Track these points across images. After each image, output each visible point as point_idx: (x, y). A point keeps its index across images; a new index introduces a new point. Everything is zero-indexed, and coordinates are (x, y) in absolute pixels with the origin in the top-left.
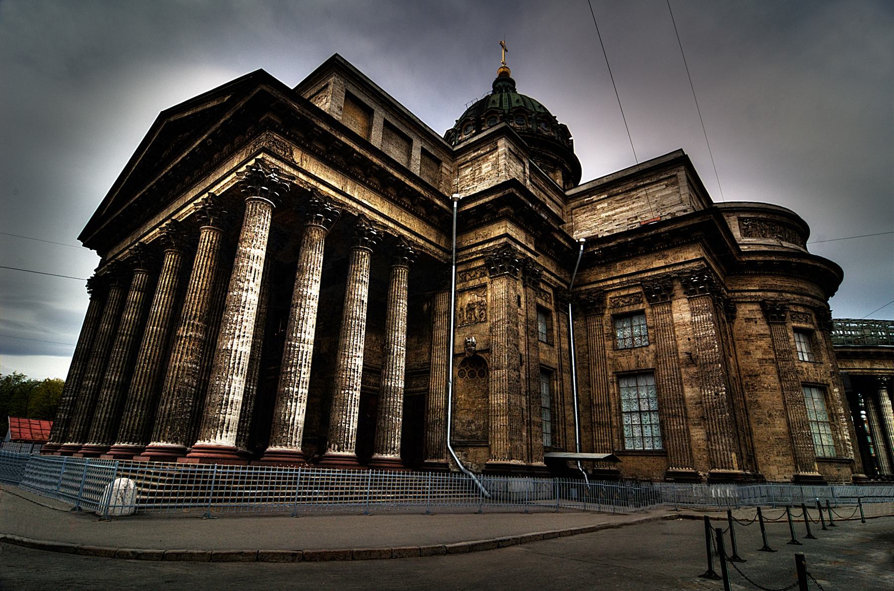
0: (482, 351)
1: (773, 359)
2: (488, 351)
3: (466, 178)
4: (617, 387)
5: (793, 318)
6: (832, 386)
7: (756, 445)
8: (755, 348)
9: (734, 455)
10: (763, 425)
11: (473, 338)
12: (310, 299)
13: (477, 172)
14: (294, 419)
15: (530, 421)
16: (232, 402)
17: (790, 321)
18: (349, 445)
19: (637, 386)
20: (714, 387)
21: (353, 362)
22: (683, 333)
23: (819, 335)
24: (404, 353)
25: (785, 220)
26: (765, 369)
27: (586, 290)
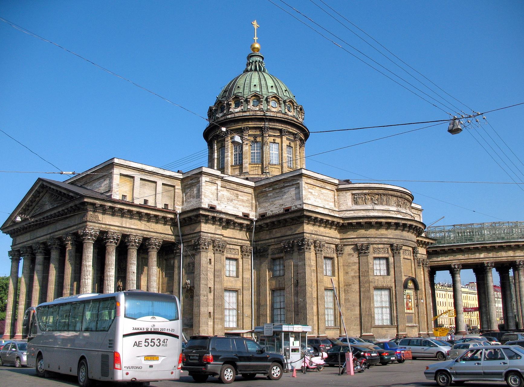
2: (193, 287)
10: (349, 311)
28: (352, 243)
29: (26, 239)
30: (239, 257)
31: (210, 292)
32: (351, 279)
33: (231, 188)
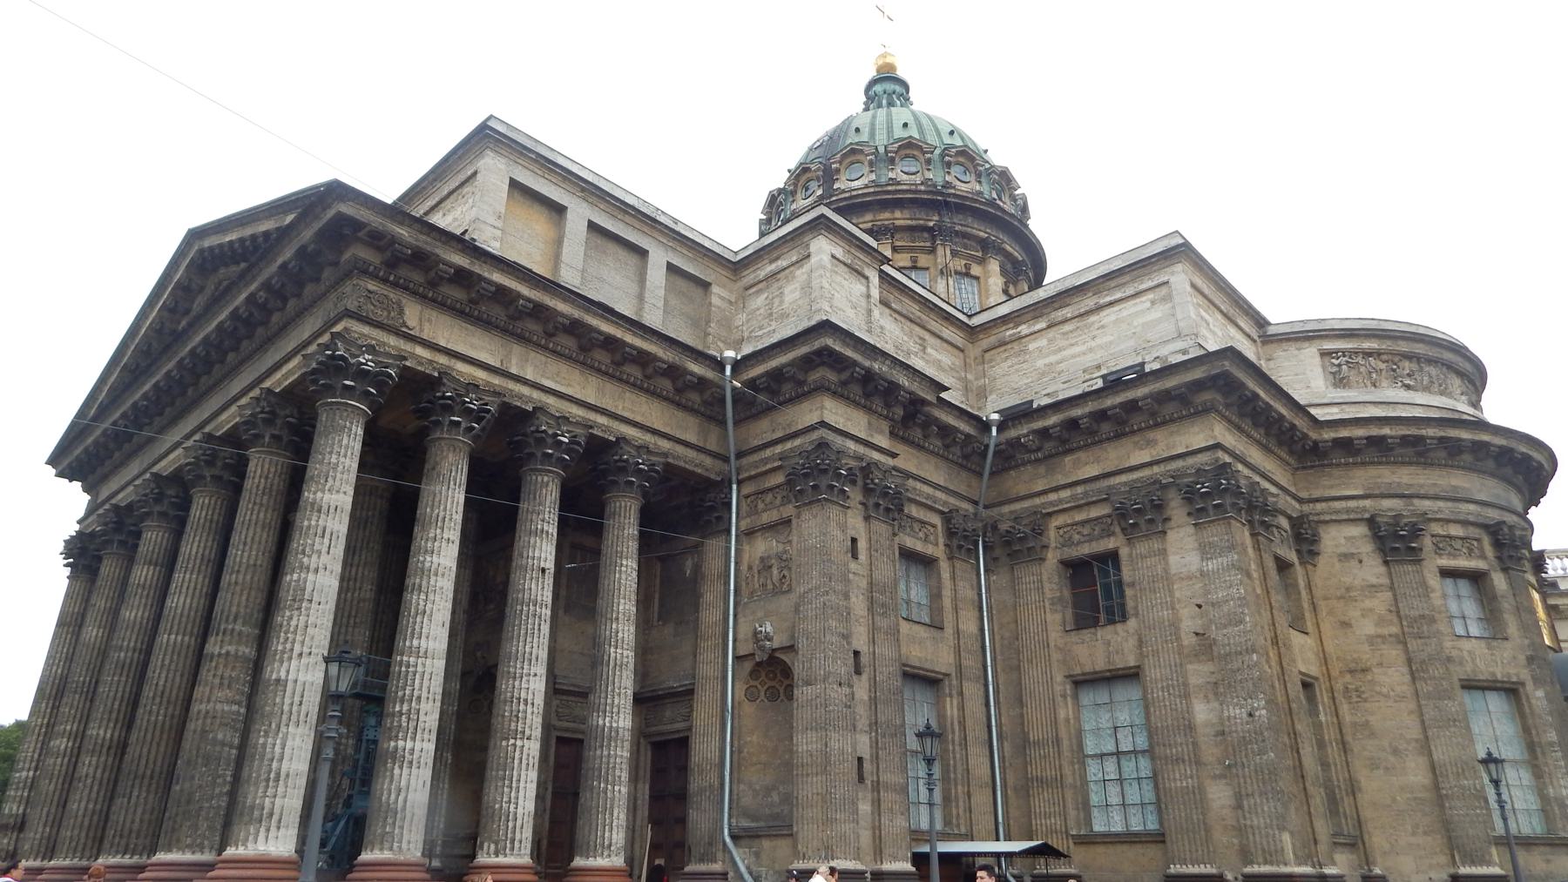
0: (781, 649)
1: (1396, 636)
2: (791, 648)
3: (758, 313)
4: (1073, 704)
5: (1440, 549)
6: (1530, 686)
7: (1367, 813)
8: (1359, 613)
9: (1286, 837)
11: (768, 624)
12: (436, 575)
13: (777, 301)
14: (405, 801)
15: (878, 782)
16: (288, 775)
17: (1433, 555)
18: (517, 845)
19: (1111, 702)
20: (1245, 700)
22: (1189, 593)
25: (1420, 349)
26: (1381, 655)
27: (1011, 512)
28: (1352, 517)
30: (937, 550)
31: (858, 672)
32: (1366, 647)
33: (905, 312)
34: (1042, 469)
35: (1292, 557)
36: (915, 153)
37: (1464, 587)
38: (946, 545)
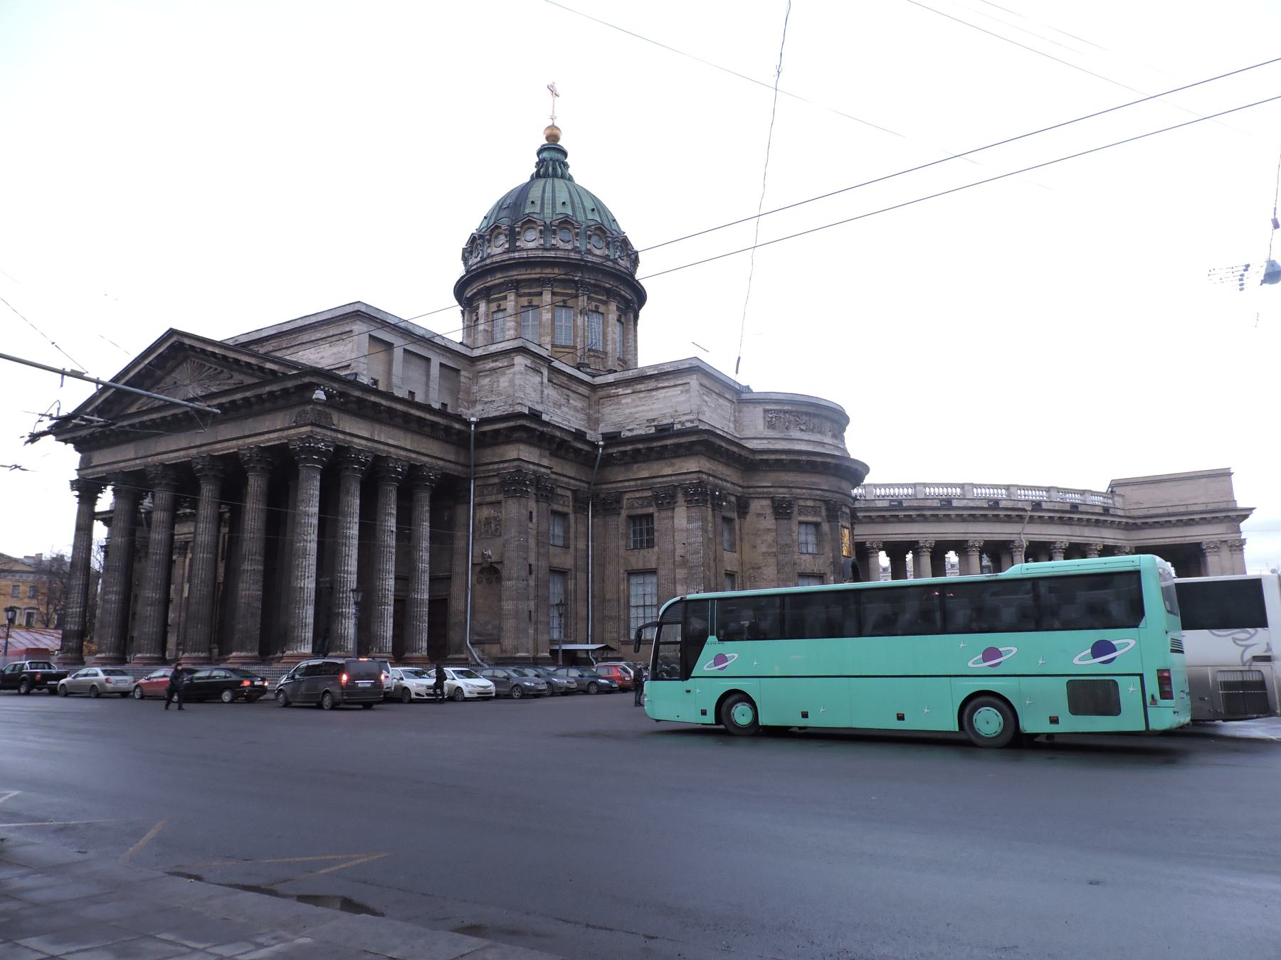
2: (501, 562)
21: (387, 583)
23: (826, 527)
24: (428, 568)
25: (811, 410)
29: (125, 457)
30: (569, 510)
33: (559, 383)
34: (623, 469)
35: (735, 515)
36: (569, 227)
37: (811, 529)
38: (574, 506)
